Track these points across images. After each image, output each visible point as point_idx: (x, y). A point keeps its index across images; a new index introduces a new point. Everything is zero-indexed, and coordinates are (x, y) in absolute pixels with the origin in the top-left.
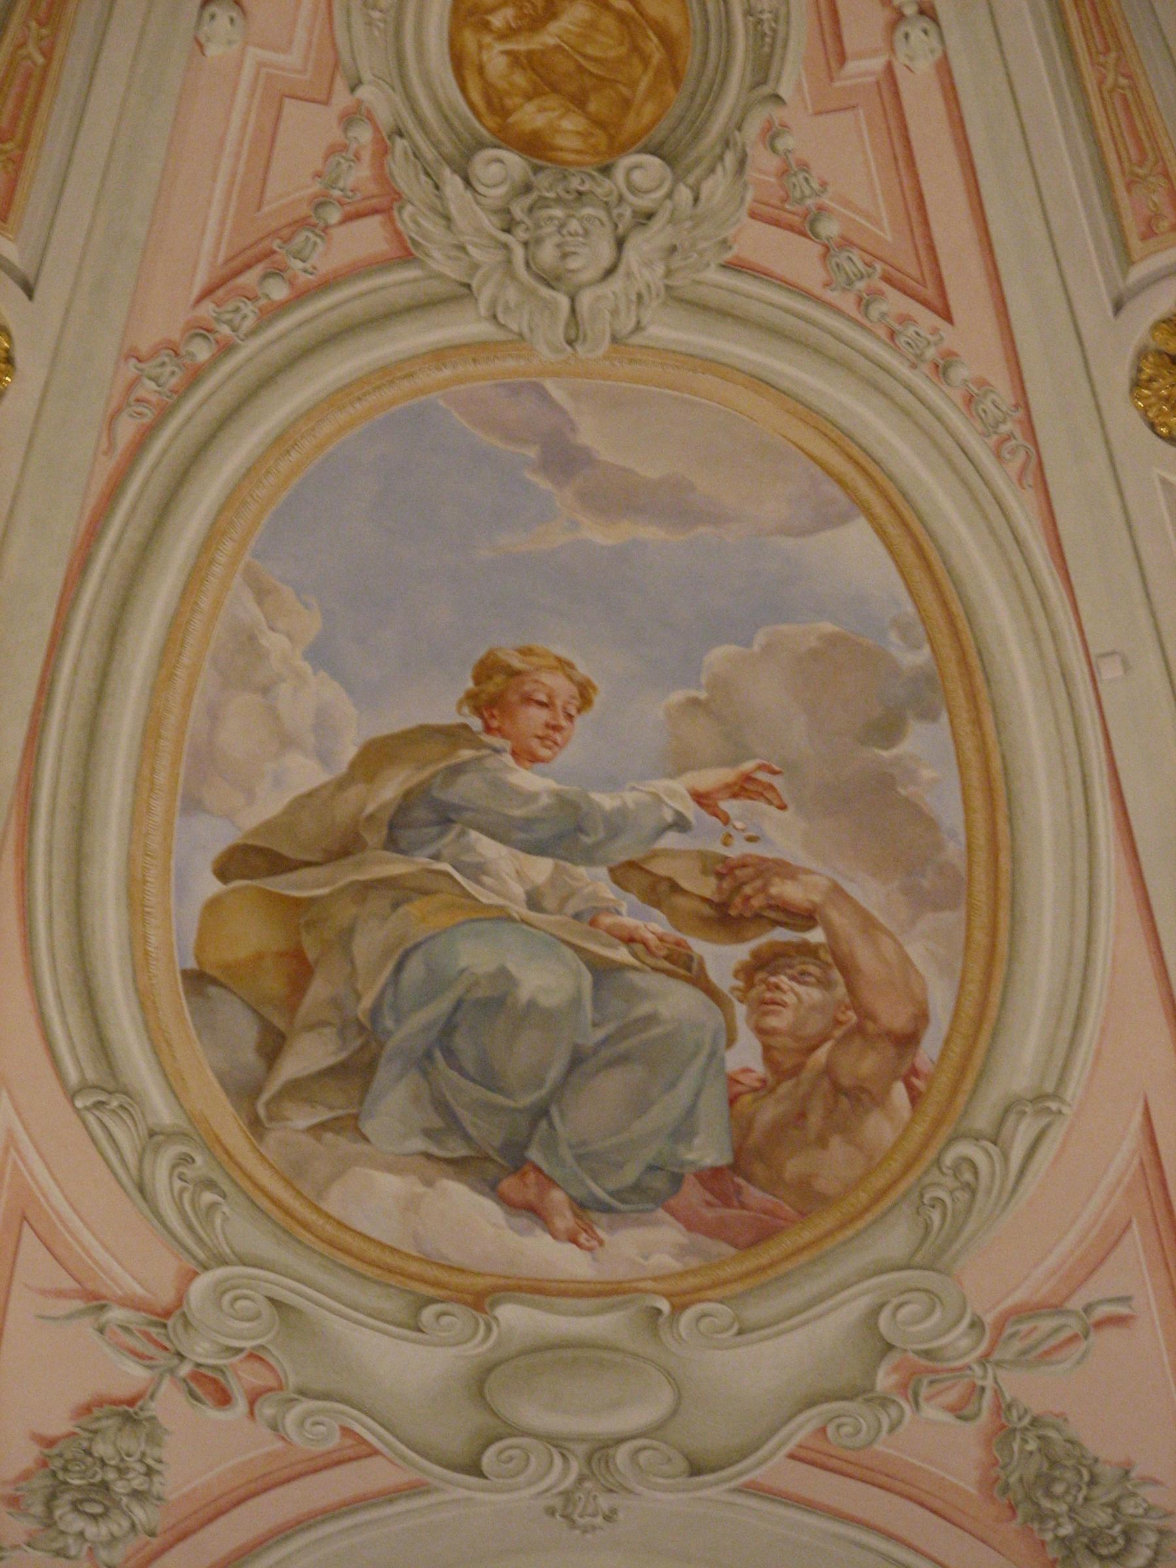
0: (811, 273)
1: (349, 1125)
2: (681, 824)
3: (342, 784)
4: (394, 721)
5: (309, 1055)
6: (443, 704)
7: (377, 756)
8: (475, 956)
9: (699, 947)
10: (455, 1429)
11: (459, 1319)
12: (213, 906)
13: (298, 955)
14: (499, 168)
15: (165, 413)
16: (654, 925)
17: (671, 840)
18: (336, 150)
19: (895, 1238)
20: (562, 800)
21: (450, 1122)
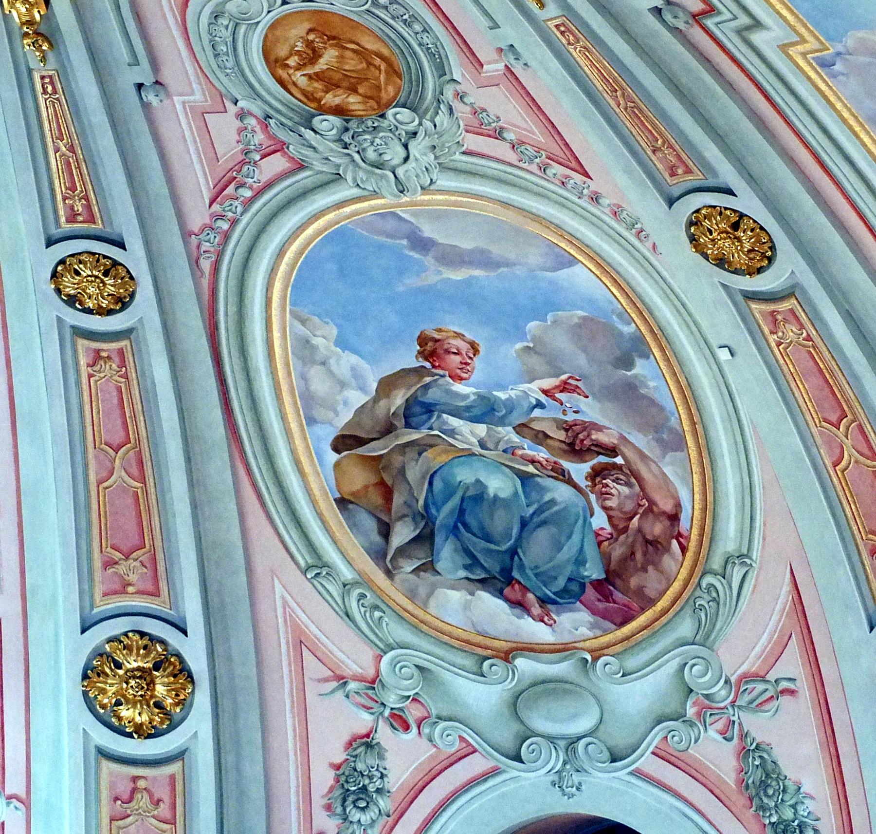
0: (511, 157)
1: (429, 567)
2: (539, 405)
3: (375, 400)
4: (388, 370)
5: (403, 533)
6: (409, 358)
7: (387, 385)
8: (464, 475)
9: (566, 465)
10: (505, 736)
11: (500, 668)
12: (337, 465)
13: (382, 484)
14: (328, 124)
15: (220, 255)
16: (542, 454)
17: (537, 413)
18: (240, 131)
19: (685, 628)
20: (481, 397)
21: (473, 563)
